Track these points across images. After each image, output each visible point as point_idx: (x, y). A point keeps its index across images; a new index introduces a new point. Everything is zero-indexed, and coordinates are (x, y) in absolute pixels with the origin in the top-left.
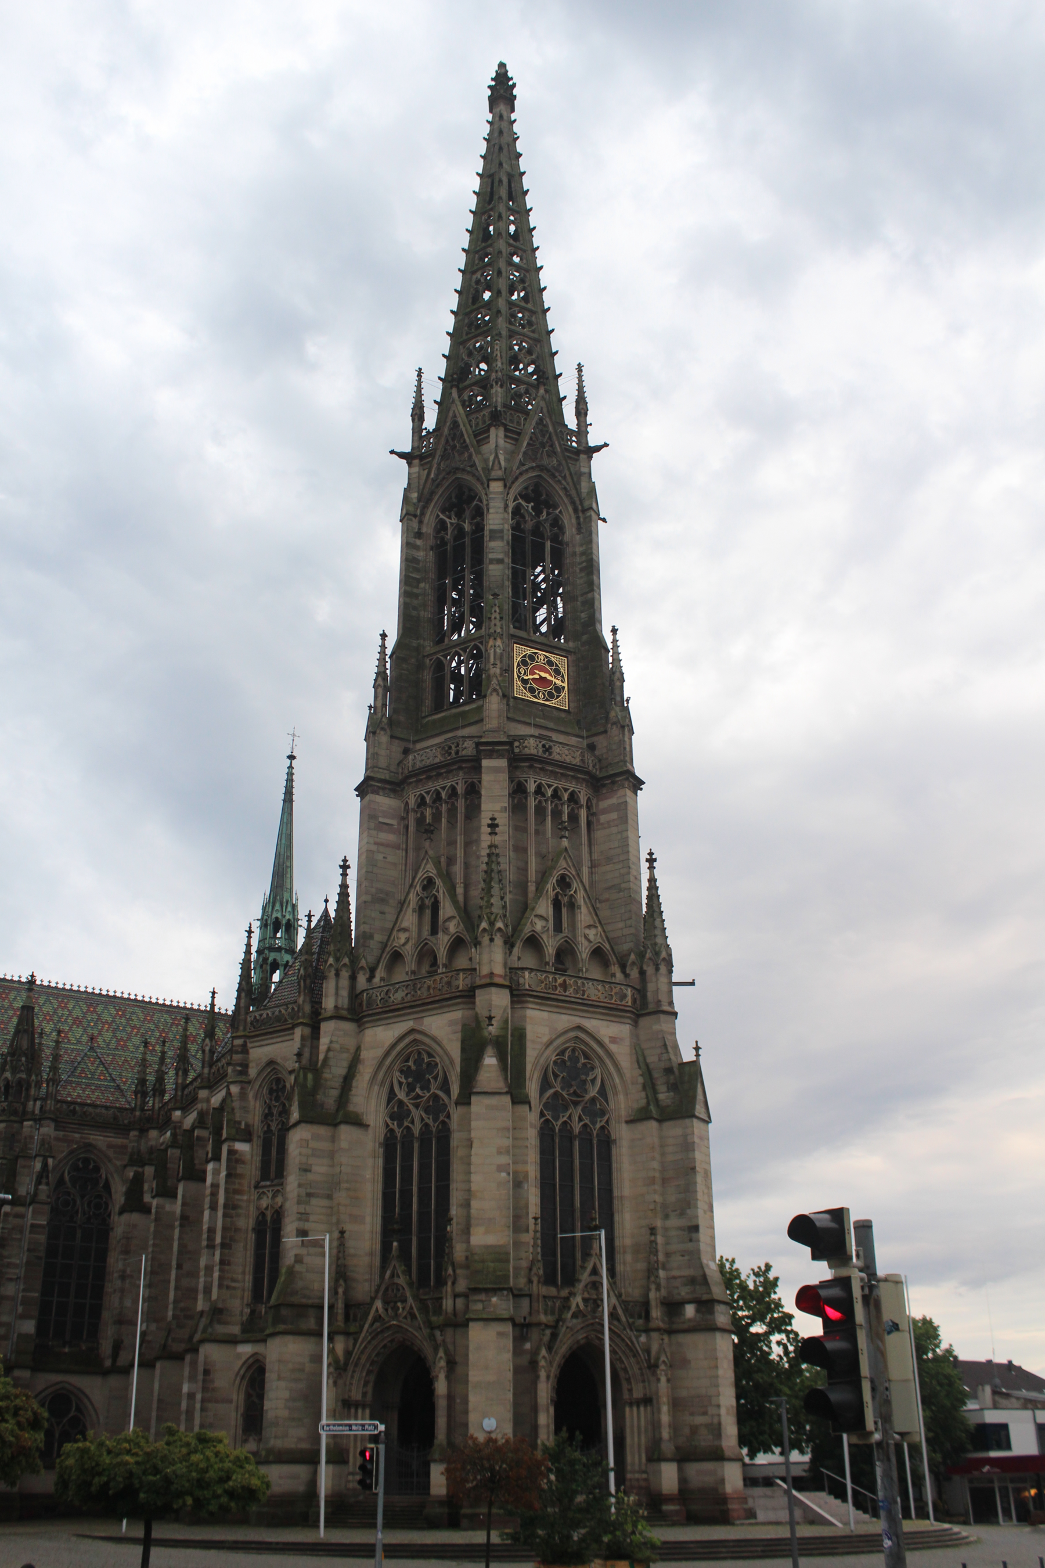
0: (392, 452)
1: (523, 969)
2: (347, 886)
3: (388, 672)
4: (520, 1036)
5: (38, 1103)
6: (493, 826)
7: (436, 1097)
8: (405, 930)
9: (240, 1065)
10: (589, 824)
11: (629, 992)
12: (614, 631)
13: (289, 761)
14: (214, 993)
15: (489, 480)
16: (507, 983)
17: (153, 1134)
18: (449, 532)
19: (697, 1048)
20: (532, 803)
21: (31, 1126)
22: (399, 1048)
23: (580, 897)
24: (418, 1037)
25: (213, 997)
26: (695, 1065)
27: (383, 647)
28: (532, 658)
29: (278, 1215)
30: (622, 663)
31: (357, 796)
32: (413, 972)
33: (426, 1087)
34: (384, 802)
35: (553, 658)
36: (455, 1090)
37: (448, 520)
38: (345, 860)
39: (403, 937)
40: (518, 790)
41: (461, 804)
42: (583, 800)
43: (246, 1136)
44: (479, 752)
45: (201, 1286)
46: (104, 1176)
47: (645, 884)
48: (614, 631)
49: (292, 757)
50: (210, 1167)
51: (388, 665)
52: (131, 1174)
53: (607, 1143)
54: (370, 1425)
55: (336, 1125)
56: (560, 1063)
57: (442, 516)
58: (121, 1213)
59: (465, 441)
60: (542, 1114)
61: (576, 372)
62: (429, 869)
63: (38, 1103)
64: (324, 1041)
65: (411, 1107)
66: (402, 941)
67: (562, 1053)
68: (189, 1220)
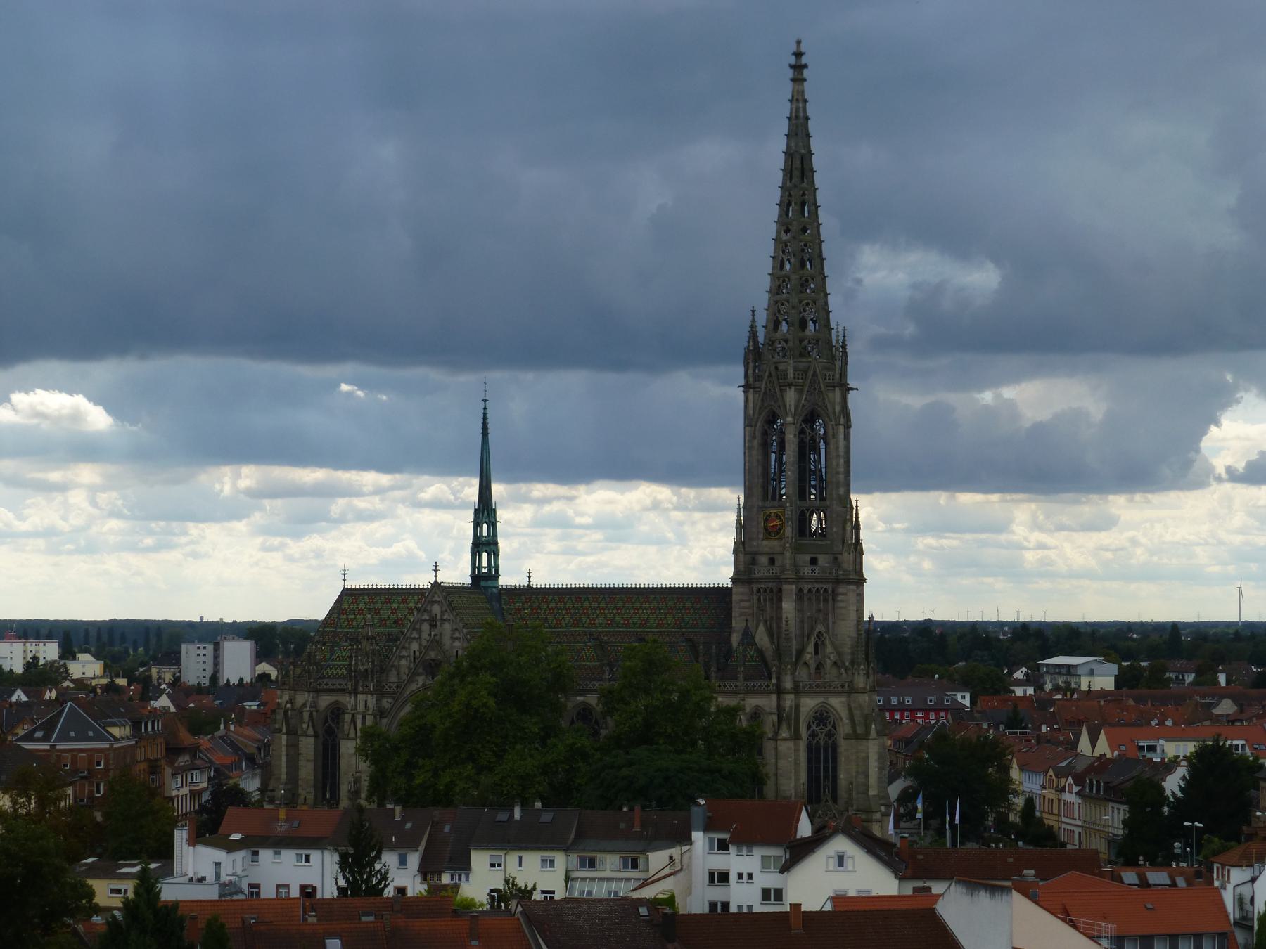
8: (809, 653)
12: (857, 501)
24: (825, 705)
33: (825, 725)
48: (857, 501)
49: (485, 401)
57: (803, 426)
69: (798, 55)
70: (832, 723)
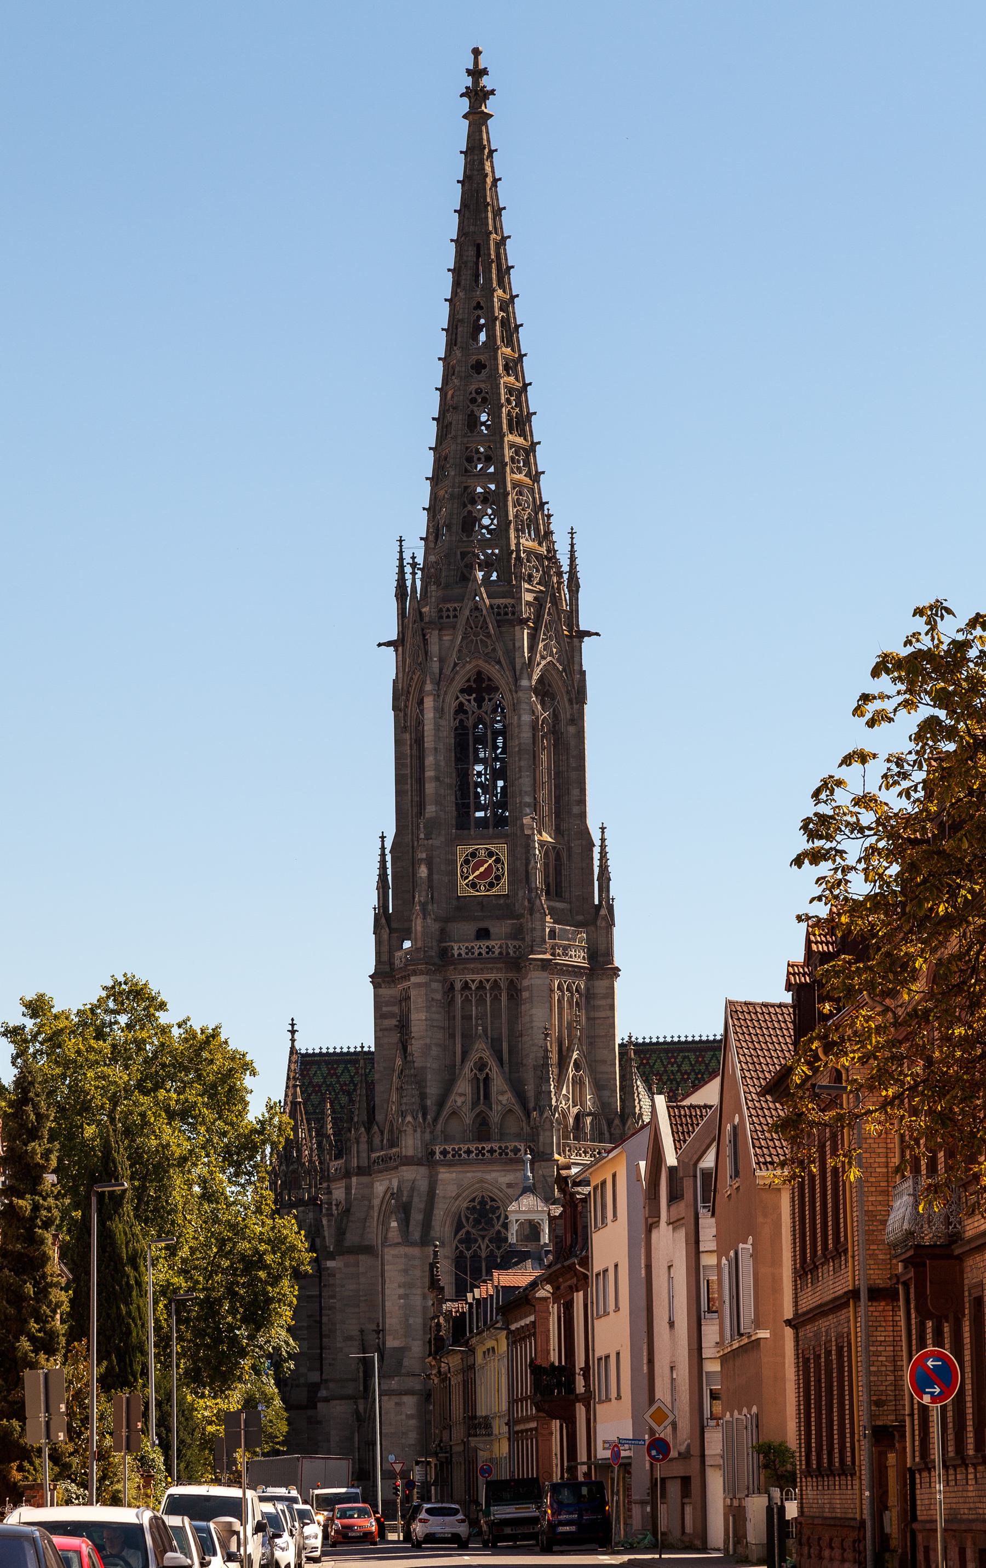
0: (380, 645)
20: (459, 1000)
27: (383, 848)
28: (473, 855)
56: (472, 1210)
60: (457, 1248)
67: (473, 1200)
69: (477, 73)
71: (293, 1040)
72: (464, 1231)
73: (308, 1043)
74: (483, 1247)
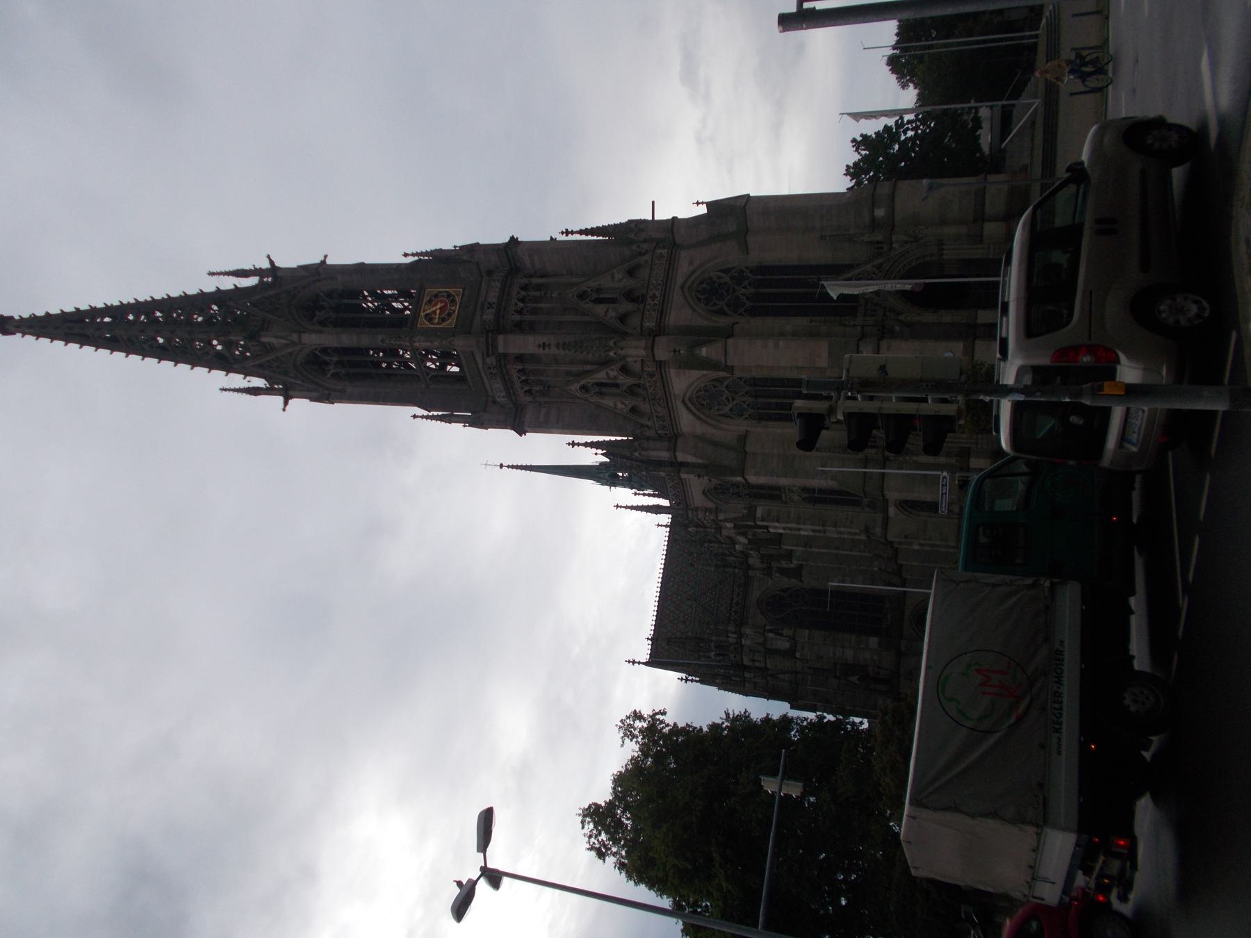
0: (284, 410)
1: (641, 327)
2: (586, 443)
3: (440, 413)
4: (687, 331)
5: (730, 635)
6: (544, 346)
7: (727, 387)
9: (706, 512)
10: (542, 276)
11: (659, 251)
12: (406, 255)
13: (504, 468)
14: (658, 525)
15: (300, 343)
16: (652, 338)
17: (751, 561)
18: (340, 371)
19: (698, 203)
20: (528, 317)
21: (745, 639)
22: (695, 411)
23: (593, 284)
25: (661, 526)
26: (710, 205)
27: (423, 417)
29: (805, 489)
30: (429, 250)
31: (525, 435)
32: (644, 399)
34: (528, 417)
35: (426, 299)
36: (722, 374)
37: (331, 372)
38: (569, 444)
39: (620, 406)
40: (519, 327)
41: (529, 367)
42: (525, 281)
43: (752, 510)
44: (493, 354)
45: (851, 537)
46: (778, 592)
47: (583, 237)
48: (406, 255)
49: (501, 466)
50: (772, 530)
51: (435, 413)
52: (778, 575)
53: (762, 269)
54: (943, 481)
55: (746, 452)
57: (329, 376)
58: (801, 581)
59: (272, 360)
60: (741, 314)
61: (215, 277)
62: (575, 387)
63: (730, 635)
64: (690, 459)
65: (735, 403)
66: (623, 406)
68: (807, 542)
70: (715, 384)
71: (639, 663)
72: (725, 308)
73: (645, 657)
74: (744, 291)
